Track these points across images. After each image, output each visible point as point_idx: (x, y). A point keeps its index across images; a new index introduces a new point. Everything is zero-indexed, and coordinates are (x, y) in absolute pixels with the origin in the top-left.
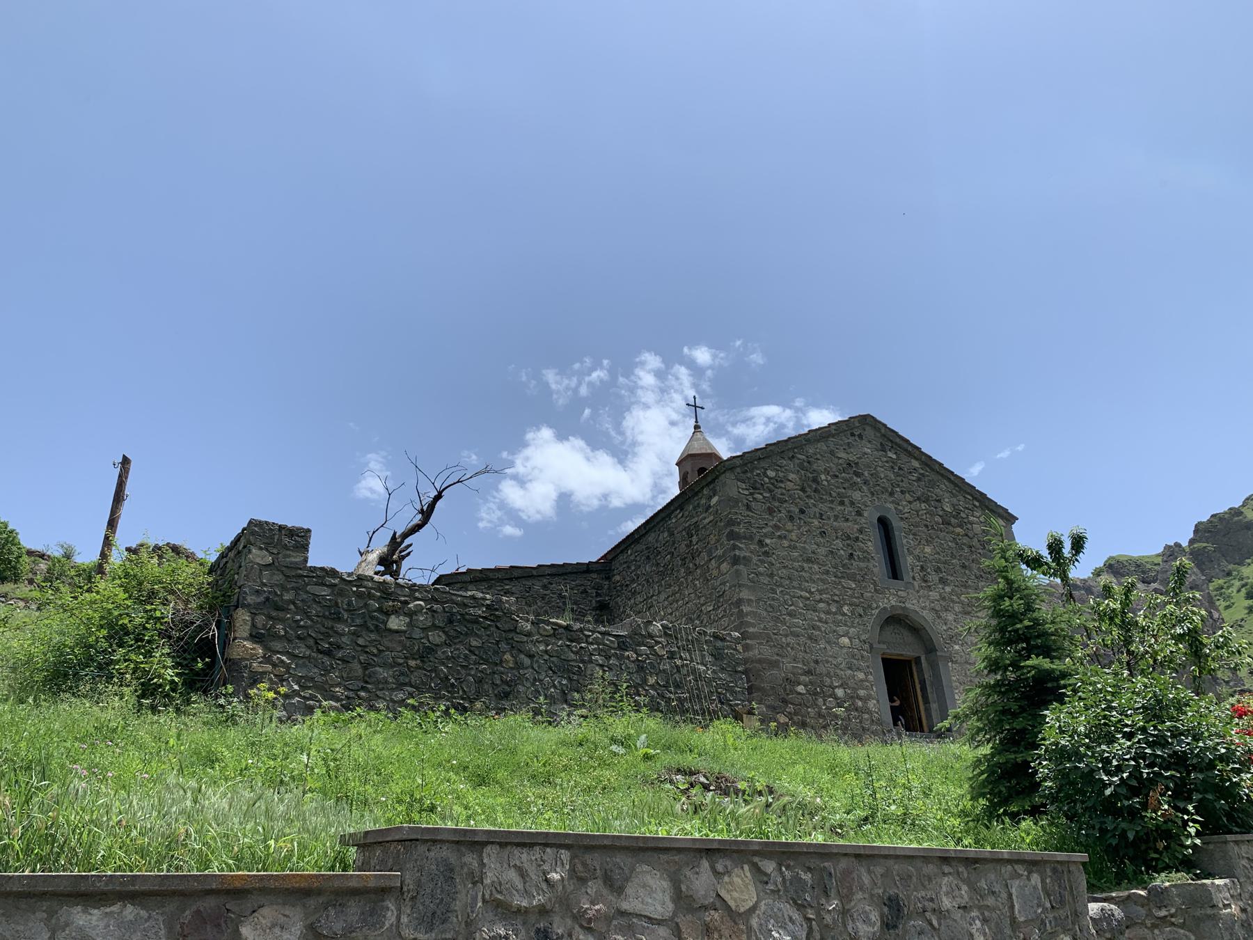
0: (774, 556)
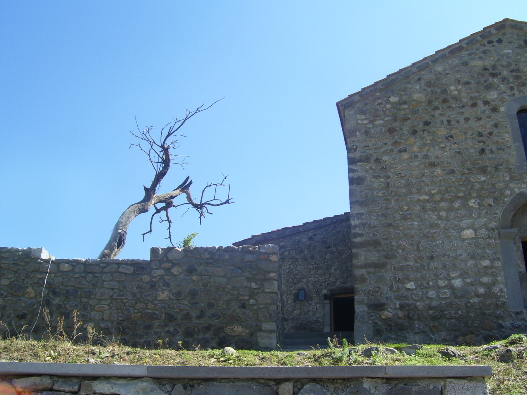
0: (392, 170)
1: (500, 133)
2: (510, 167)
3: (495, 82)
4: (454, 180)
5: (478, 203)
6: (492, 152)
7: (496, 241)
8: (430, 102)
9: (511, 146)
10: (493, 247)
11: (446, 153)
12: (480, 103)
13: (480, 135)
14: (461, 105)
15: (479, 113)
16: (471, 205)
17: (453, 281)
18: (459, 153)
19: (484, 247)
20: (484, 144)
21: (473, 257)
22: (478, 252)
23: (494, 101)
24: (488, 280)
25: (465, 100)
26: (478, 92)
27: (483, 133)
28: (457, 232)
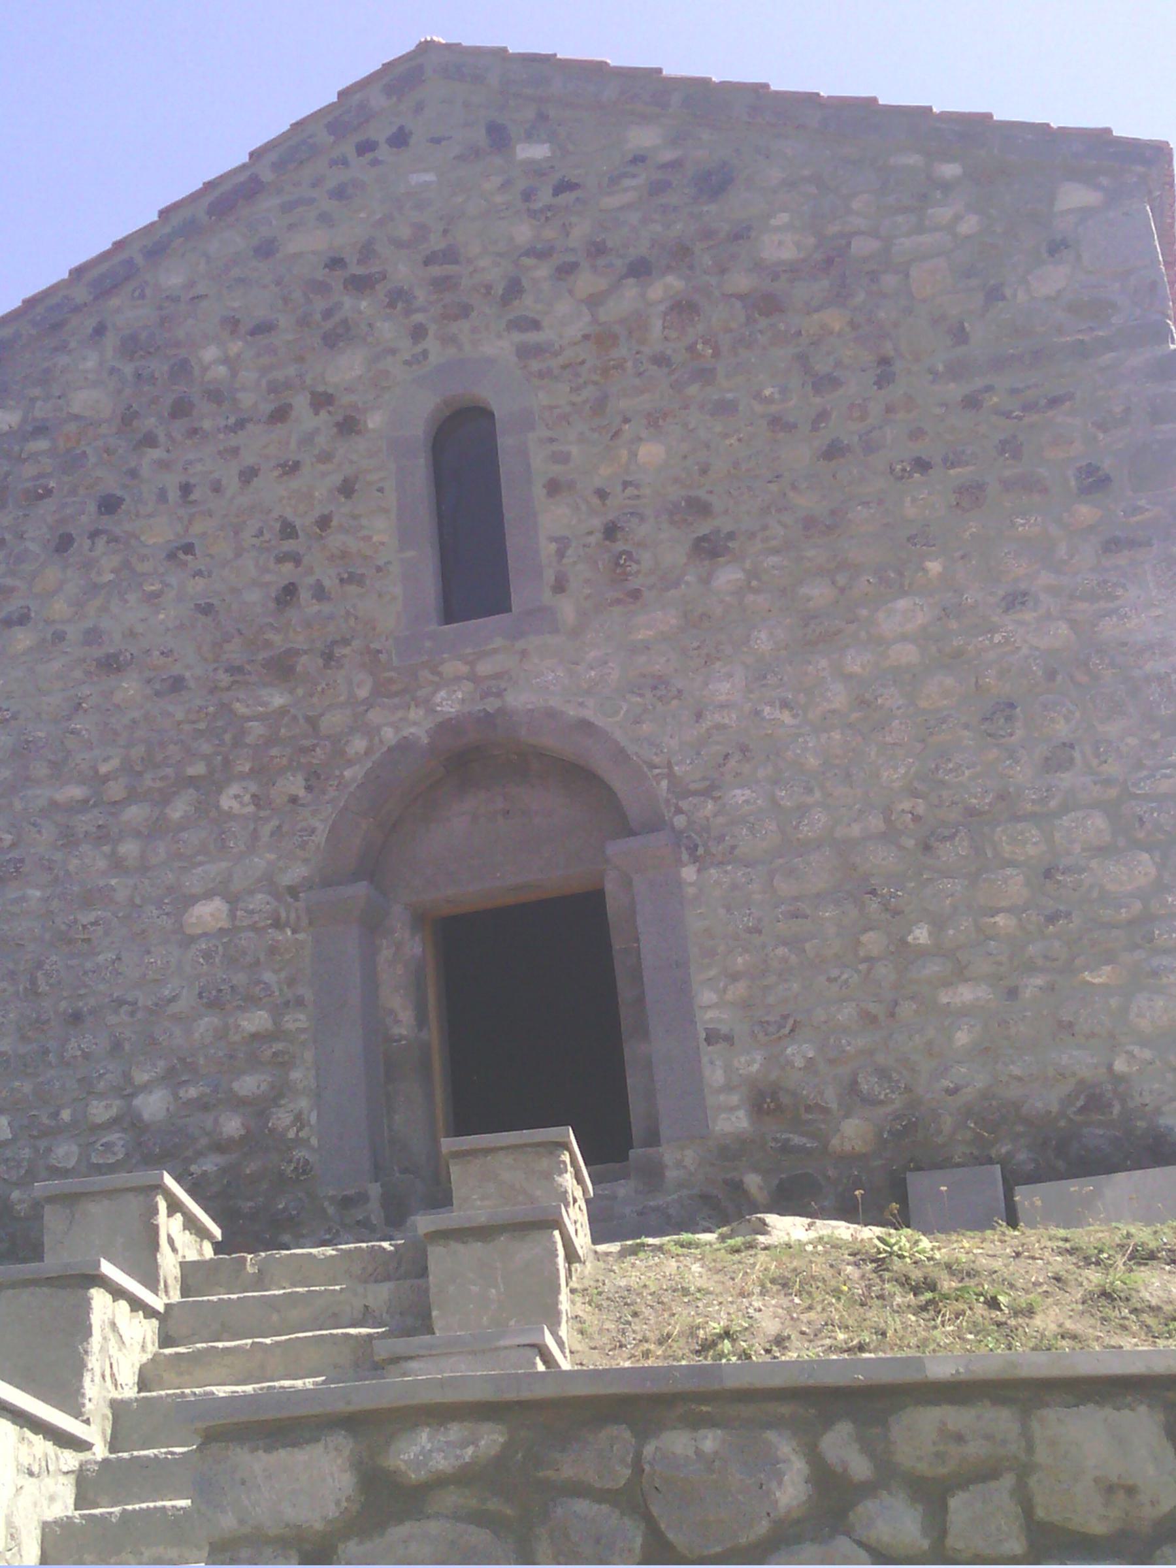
1: (355, 517)
2: (375, 646)
3: (360, 312)
4: (180, 716)
5: (254, 796)
6: (320, 593)
7: (297, 936)
8: (128, 418)
9: (389, 563)
10: (287, 957)
11: (162, 616)
12: (301, 403)
13: (288, 530)
14: (232, 420)
15: (293, 445)
16: (226, 808)
17: (138, 1102)
18: (207, 610)
19: (258, 962)
20: (297, 567)
21: (215, 1004)
22: (235, 982)
23: (349, 390)
24: (259, 1087)
25: (247, 399)
26: (300, 359)
27: (298, 523)
28: (167, 914)
